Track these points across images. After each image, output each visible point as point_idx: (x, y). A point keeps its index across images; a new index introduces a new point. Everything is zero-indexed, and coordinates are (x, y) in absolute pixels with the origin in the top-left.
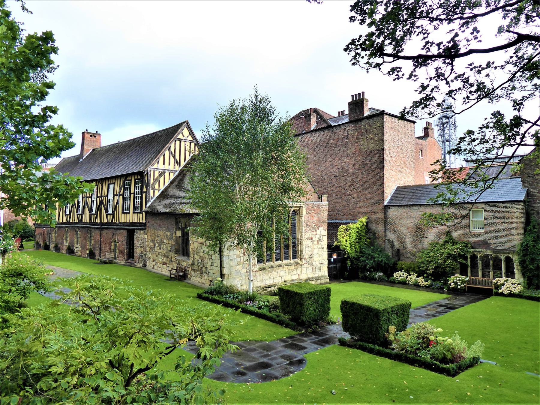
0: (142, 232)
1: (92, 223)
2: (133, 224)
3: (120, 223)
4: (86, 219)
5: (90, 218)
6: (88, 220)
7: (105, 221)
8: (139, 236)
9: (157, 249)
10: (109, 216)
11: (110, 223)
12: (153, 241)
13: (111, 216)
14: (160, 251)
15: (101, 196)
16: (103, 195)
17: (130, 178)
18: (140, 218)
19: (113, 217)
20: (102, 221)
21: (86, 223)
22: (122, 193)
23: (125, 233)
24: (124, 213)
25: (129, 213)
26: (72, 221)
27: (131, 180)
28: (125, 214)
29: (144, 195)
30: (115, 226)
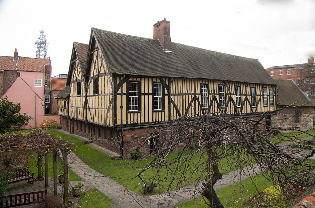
0: (275, 116)
2: (269, 112)
5: (236, 110)
6: (233, 112)
7: (250, 112)
8: (274, 117)
10: (253, 109)
11: (254, 113)
13: (255, 109)
14: (286, 123)
15: (246, 95)
16: (247, 94)
17: (266, 87)
18: (273, 109)
19: (257, 109)
20: (248, 112)
21: (232, 115)
22: (262, 94)
24: (264, 106)
25: (267, 106)
27: (267, 88)
28: (265, 107)
29: (274, 96)
30: (258, 114)
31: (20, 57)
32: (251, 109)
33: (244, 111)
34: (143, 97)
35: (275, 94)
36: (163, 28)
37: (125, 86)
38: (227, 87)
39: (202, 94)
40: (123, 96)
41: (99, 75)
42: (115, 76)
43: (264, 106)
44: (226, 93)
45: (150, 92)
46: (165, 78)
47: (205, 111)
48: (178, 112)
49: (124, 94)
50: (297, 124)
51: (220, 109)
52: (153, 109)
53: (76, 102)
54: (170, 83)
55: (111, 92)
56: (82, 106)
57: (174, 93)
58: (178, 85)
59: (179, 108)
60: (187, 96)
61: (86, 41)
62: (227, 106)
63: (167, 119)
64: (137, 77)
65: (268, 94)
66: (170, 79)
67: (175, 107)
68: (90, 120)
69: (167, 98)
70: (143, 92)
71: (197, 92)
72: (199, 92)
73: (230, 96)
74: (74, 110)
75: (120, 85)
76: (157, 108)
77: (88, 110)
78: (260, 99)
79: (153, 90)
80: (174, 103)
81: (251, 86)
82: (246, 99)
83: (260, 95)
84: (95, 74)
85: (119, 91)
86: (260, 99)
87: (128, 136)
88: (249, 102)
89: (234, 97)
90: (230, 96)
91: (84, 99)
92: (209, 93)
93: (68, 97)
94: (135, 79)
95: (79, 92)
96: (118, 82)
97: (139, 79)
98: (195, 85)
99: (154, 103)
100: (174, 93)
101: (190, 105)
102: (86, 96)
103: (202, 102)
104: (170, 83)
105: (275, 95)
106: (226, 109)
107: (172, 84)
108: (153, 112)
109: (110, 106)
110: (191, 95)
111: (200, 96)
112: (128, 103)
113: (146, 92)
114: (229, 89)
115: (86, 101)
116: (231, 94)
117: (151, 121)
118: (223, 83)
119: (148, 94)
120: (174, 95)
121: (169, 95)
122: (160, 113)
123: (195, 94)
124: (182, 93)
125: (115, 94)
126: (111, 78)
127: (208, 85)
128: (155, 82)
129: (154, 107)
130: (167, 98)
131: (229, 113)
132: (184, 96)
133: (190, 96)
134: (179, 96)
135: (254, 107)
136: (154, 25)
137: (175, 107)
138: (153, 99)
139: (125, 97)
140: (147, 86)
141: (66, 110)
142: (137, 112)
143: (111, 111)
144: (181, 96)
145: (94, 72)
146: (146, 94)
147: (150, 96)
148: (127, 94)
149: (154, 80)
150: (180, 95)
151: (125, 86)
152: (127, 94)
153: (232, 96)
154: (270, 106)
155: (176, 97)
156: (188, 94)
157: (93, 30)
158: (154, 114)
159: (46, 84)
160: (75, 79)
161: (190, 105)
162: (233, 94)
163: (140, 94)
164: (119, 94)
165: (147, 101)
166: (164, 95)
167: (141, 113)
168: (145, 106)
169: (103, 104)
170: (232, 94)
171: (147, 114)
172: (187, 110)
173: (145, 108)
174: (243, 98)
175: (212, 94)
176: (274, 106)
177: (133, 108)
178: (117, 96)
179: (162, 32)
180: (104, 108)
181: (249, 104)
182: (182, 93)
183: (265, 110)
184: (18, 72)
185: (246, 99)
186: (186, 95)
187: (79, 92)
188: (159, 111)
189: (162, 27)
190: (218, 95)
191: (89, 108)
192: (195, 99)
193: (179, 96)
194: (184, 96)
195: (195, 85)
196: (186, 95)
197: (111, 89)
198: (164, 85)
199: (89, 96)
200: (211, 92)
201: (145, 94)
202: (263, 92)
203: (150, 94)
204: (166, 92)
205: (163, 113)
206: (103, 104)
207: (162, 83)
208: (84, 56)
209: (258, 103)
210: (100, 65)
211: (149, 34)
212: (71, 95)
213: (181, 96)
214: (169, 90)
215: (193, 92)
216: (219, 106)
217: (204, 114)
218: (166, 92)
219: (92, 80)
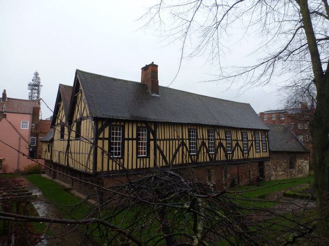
1: (227, 161)
2: (263, 158)
3: (254, 158)
4: (221, 156)
5: (226, 156)
8: (268, 165)
9: (279, 169)
10: (245, 154)
12: (275, 166)
15: (237, 140)
18: (266, 155)
19: (249, 154)
20: (239, 158)
23: (257, 164)
24: (257, 152)
25: (260, 152)
26: (201, 159)
31: (8, 98)
32: (243, 155)
33: (235, 157)
34: (126, 142)
35: (268, 139)
36: (151, 71)
37: (107, 130)
38: (217, 132)
39: (189, 139)
40: (105, 141)
41: (82, 119)
42: (96, 120)
43: (257, 152)
44: (216, 138)
45: (135, 137)
46: (152, 122)
47: (193, 157)
48: (164, 158)
49: (106, 139)
50: (291, 170)
51: (209, 155)
52: (137, 155)
53: (59, 145)
54: (155, 128)
55: (93, 137)
56: (65, 150)
57: (161, 138)
58: (164, 130)
59: (165, 154)
60: (174, 141)
61: (71, 83)
62: (216, 152)
63: (152, 165)
64: (120, 121)
65: (260, 139)
66: (156, 124)
67: (161, 152)
68: (71, 165)
69: (152, 143)
70: (126, 137)
71: (184, 137)
72: (187, 138)
73: (220, 142)
74: (57, 154)
75: (102, 129)
76: (142, 154)
77: (70, 154)
78: (252, 145)
79: (138, 135)
80: (160, 149)
81: (242, 131)
82: (237, 145)
83: (252, 140)
84: (78, 117)
85: (101, 136)
86: (252, 145)
87: (108, 184)
88: (240, 148)
89: (224, 142)
90: (220, 142)
91: (66, 142)
92: (197, 139)
93: (52, 141)
94: (118, 124)
95: (62, 136)
96: (100, 126)
97: (122, 124)
98: (182, 130)
99: (138, 149)
100: (161, 138)
101: (177, 150)
102: (69, 140)
103: (190, 147)
104: (155, 128)
105: (268, 141)
106: (215, 154)
107: (158, 129)
108: (137, 158)
109: (91, 151)
110: (178, 140)
111: (187, 141)
112: (110, 149)
113: (130, 137)
114: (219, 134)
115: (69, 145)
116: (220, 139)
117: (134, 167)
118: (213, 128)
119: (132, 139)
120: (160, 140)
121: (155, 140)
122: (145, 159)
123: (183, 139)
124: (168, 138)
125: (97, 138)
126: (93, 122)
127: (197, 130)
128: (140, 127)
129: (138, 153)
130: (152, 143)
131: (219, 160)
132: (171, 141)
133: (177, 141)
134: (165, 142)
135: (246, 153)
136: (142, 69)
137: (161, 152)
138: (138, 144)
139: (106, 142)
140: (131, 131)
141: (49, 154)
142: (120, 158)
143: (92, 157)
144: (168, 142)
145: (77, 116)
146: (130, 139)
147: (135, 142)
148: (109, 139)
149: (139, 125)
150: (166, 140)
151: (107, 130)
152: (109, 139)
153: (222, 141)
154: (263, 152)
155: (162, 142)
156: (175, 140)
157: (78, 72)
158: (139, 160)
159: (33, 126)
160: (59, 121)
161: (177, 150)
162: (223, 140)
163: (124, 139)
164: (101, 139)
165: (130, 147)
166: (149, 140)
167: (124, 159)
168: (128, 152)
169: (84, 149)
170: (222, 139)
171: (131, 161)
172: (174, 157)
173: (128, 154)
174: (234, 143)
175: (201, 139)
176: (267, 151)
177: (116, 153)
178: (98, 141)
179: (150, 76)
180: (85, 154)
181: (241, 149)
182: (168, 138)
183: (257, 156)
184: (4, 113)
185: (237, 145)
186: (172, 140)
187: (62, 136)
188: (143, 157)
189: (149, 71)
190: (207, 141)
191: (71, 153)
192: (183, 144)
193: (165, 142)
194: (171, 141)
195: (182, 130)
196: (172, 140)
197: (92, 133)
198: (149, 130)
199: (71, 140)
200: (199, 138)
201: (128, 139)
202: (255, 138)
203: (134, 139)
204: (152, 137)
205: (148, 159)
206: (84, 149)
207: (148, 128)
208: (68, 98)
209: (250, 149)
210: (82, 109)
211: (136, 77)
212: (55, 139)
213: (168, 142)
214: (154, 135)
215: (181, 137)
216: (208, 151)
217: (192, 160)
218: (152, 137)
219: (75, 124)
